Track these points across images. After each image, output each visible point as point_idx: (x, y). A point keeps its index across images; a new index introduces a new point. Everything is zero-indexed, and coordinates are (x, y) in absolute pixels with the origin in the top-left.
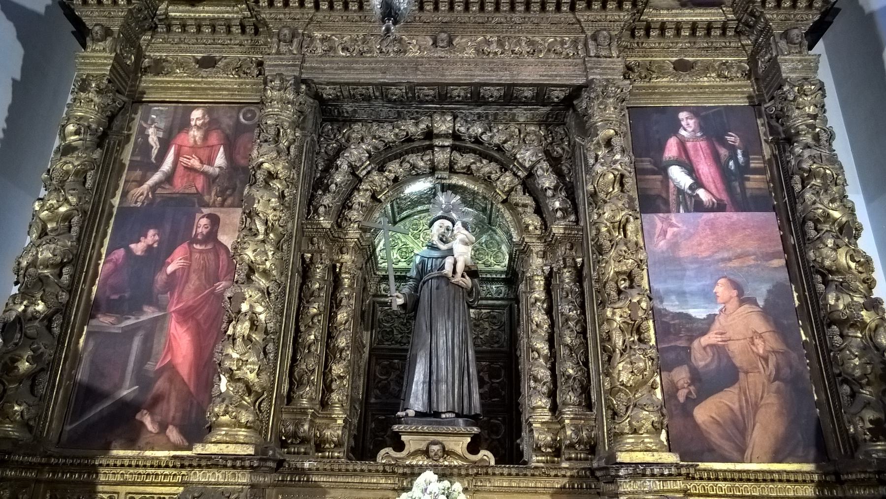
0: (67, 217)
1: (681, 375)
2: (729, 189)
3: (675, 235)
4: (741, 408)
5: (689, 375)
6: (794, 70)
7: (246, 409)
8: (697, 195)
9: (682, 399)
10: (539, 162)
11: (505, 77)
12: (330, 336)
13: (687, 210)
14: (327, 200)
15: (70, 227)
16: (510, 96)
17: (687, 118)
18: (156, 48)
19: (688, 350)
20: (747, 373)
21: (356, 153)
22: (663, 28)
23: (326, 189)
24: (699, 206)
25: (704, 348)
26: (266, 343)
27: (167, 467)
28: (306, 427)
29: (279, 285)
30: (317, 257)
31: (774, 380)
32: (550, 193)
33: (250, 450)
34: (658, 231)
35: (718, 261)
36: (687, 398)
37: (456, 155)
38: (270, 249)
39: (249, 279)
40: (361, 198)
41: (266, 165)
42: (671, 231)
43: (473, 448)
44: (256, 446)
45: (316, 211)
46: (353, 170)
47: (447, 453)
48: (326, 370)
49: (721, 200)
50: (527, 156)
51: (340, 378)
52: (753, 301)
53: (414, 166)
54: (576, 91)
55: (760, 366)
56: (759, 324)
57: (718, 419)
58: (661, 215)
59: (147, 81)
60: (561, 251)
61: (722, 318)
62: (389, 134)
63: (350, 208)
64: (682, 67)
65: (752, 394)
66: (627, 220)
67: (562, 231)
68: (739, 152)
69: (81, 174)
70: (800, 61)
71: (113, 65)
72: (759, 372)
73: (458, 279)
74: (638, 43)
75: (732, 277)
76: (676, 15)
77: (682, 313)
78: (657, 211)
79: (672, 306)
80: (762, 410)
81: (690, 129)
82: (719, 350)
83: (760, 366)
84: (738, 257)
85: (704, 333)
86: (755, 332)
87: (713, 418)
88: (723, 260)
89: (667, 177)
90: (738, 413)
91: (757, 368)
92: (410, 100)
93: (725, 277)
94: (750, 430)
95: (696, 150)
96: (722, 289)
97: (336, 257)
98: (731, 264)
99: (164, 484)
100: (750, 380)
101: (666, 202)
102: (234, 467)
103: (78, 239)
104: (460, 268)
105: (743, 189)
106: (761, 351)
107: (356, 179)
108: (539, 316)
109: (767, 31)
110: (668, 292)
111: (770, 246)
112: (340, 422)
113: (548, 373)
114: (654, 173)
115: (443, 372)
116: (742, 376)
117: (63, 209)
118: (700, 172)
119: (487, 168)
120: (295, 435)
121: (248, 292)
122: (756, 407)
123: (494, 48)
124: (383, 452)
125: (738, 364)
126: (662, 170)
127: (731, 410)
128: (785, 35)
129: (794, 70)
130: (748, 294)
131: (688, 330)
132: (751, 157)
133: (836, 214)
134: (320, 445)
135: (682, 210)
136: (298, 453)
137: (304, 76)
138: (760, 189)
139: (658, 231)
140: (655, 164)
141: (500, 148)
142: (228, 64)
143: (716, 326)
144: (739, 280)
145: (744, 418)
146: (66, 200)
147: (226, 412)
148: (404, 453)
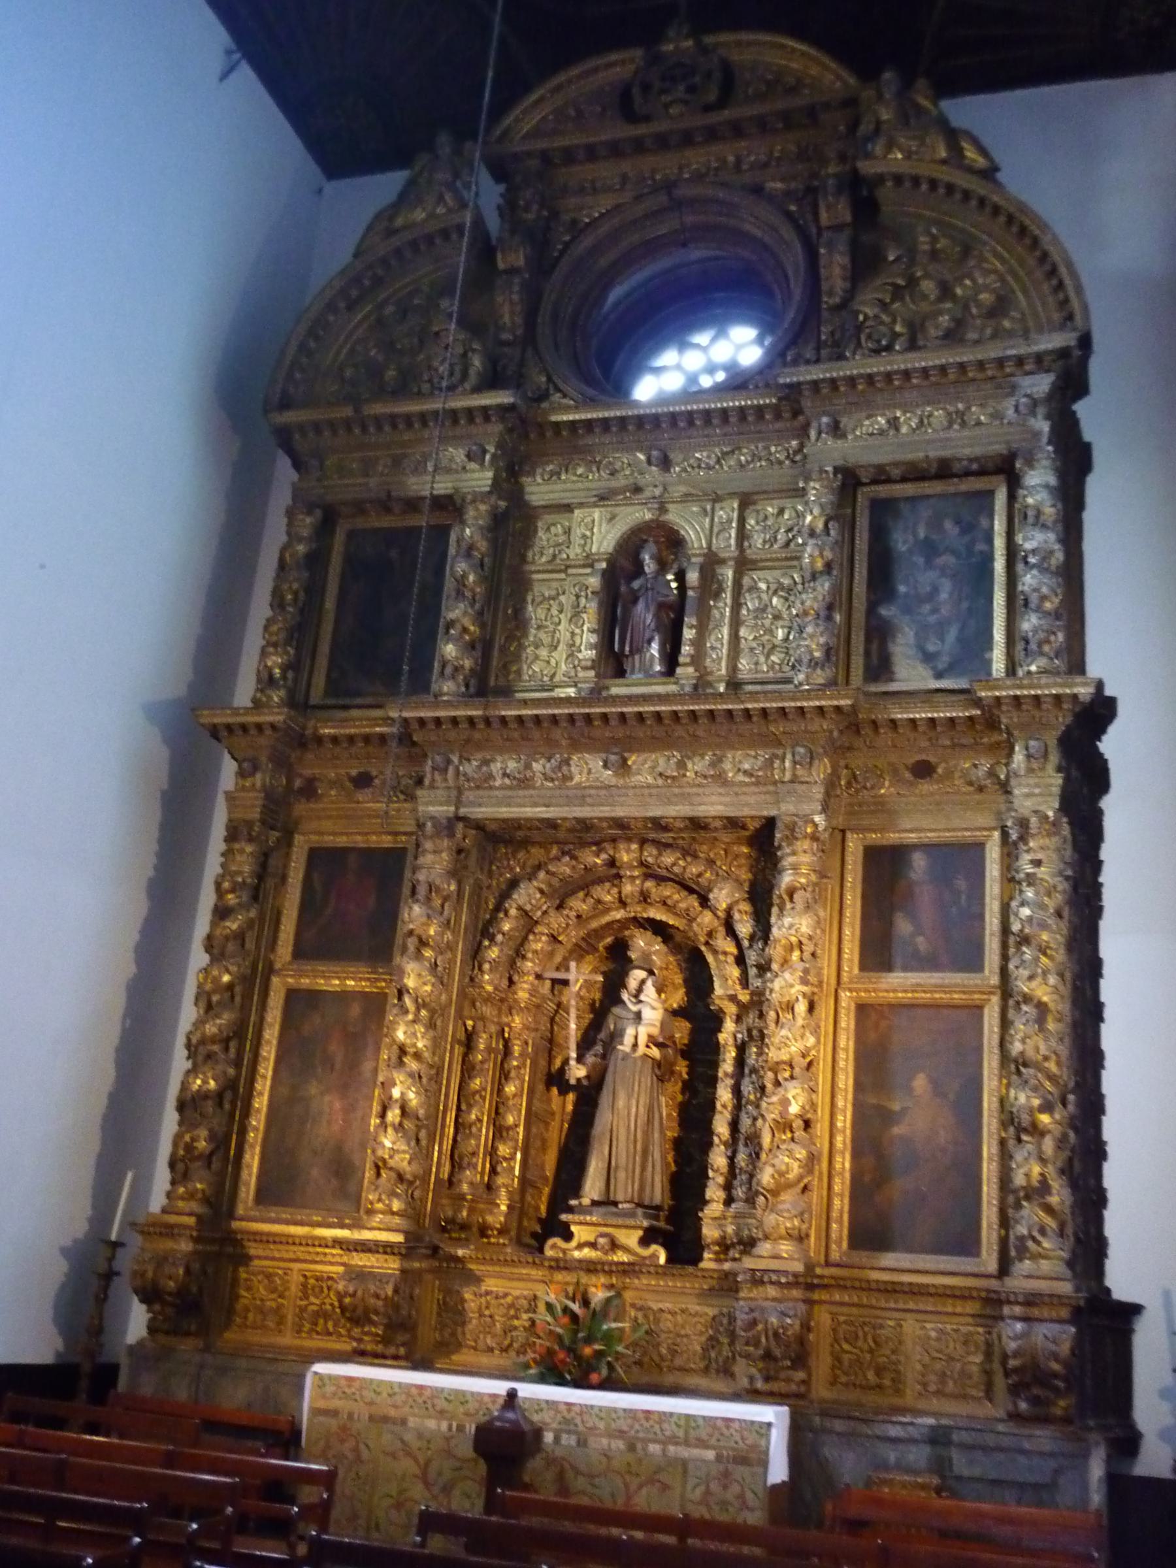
0: (230, 987)
6: (1028, 796)
7: (397, 1195)
10: (737, 902)
11: (684, 810)
12: (497, 1112)
15: (232, 997)
16: (697, 824)
18: (310, 766)
21: (526, 895)
23: (492, 939)
26: (420, 1128)
28: (465, 1213)
29: (431, 1067)
30: (480, 1024)
33: (399, 1238)
38: (420, 1029)
39: (401, 1063)
40: (538, 944)
44: (406, 1233)
45: (480, 969)
46: (524, 913)
47: (614, 1245)
48: (492, 1152)
50: (722, 897)
53: (599, 901)
54: (770, 824)
62: (564, 868)
63: (524, 957)
92: (585, 833)
97: (505, 1020)
99: (332, 1264)
102: (385, 1253)
103: (242, 1007)
107: (529, 923)
117: (226, 978)
120: (451, 1221)
121: (399, 1077)
124: (551, 1242)
134: (483, 1231)
136: (459, 1239)
147: (380, 1200)
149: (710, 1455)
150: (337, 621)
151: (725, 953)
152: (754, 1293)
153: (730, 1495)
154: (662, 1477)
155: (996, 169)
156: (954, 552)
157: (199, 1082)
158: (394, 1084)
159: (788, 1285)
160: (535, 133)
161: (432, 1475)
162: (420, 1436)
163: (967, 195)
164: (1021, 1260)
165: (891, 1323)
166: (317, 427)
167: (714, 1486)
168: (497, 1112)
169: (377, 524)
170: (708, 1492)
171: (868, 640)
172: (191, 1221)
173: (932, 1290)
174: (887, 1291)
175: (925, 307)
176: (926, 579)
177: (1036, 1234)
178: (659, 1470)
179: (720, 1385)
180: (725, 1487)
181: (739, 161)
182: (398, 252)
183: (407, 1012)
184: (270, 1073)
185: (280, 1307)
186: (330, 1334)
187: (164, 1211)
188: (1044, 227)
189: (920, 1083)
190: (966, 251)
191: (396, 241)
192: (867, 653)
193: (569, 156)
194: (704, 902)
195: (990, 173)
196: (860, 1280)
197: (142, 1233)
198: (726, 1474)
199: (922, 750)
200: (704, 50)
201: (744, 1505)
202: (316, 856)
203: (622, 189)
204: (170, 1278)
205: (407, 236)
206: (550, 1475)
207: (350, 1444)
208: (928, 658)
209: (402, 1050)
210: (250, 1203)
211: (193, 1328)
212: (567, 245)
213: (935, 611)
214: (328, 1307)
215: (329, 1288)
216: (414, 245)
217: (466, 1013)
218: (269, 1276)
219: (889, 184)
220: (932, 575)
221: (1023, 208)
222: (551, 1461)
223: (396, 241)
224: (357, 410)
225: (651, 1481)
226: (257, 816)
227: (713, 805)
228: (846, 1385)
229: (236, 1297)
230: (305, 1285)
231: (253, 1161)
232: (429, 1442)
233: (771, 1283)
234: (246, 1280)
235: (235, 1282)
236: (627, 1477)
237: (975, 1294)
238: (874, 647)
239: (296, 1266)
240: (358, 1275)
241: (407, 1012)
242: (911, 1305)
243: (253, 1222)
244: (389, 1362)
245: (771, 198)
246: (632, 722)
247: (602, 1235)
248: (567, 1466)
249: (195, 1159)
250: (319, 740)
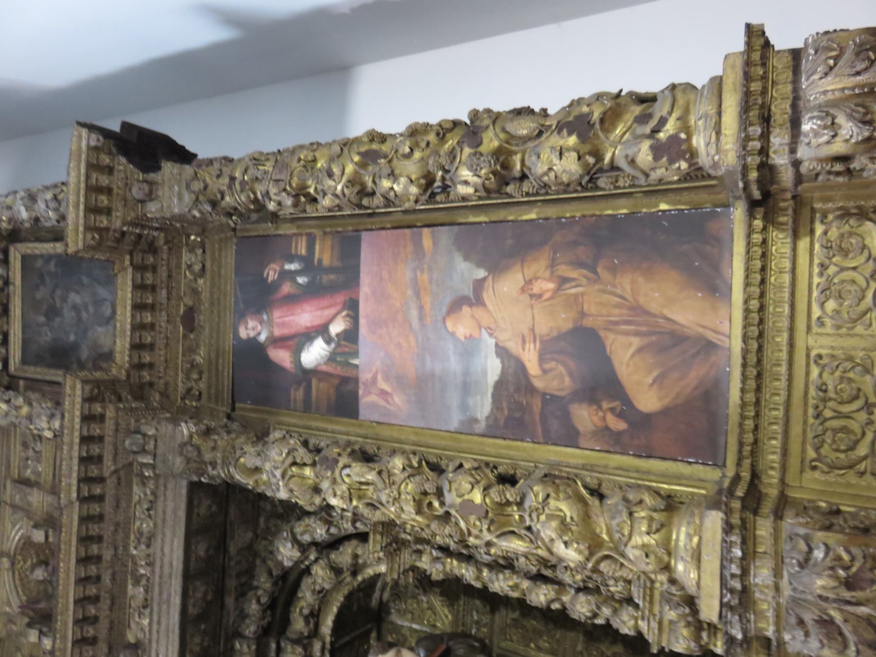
1: (585, 417)
2: (330, 289)
3: (387, 379)
4: (637, 334)
5: (585, 405)
6: (180, 197)
8: (337, 335)
9: (622, 426)
13: (356, 354)
17: (246, 328)
19: (548, 399)
20: (583, 314)
22: (137, 347)
24: (351, 336)
25: (545, 372)
31: (596, 273)
32: (333, 530)
34: (382, 402)
35: (423, 326)
36: (620, 416)
37: (290, 634)
42: (383, 385)
49: (344, 304)
52: (479, 285)
55: (573, 291)
56: (510, 284)
57: (655, 373)
58: (361, 392)
61: (503, 336)
65: (617, 311)
67: (379, 537)
68: (288, 267)
72: (583, 294)
74: (160, 378)
75: (444, 310)
77: (494, 396)
78: (354, 398)
79: (483, 407)
80: (642, 300)
81: (259, 328)
82: (549, 349)
83: (573, 291)
84: (417, 294)
85: (522, 368)
86: (523, 290)
87: (654, 381)
88: (421, 317)
89: (313, 372)
90: (646, 340)
91: (576, 296)
93: (444, 320)
94: (675, 327)
95: (283, 325)
96: (462, 326)
98: (427, 307)
100: (594, 311)
101: (345, 380)
105: (330, 270)
106: (551, 286)
110: (464, 407)
111: (405, 247)
114: (308, 388)
116: (588, 322)
118: (309, 325)
119: (306, 598)
122: (638, 310)
125: (569, 325)
126: (307, 375)
127: (640, 350)
129: (180, 197)
130: (468, 291)
131: (518, 390)
132: (293, 251)
135: (355, 362)
138: (332, 247)
139: (382, 402)
140: (299, 384)
143: (514, 346)
144: (448, 300)
145: (655, 333)
151: (356, 556)
159: (748, 542)
164: (693, 154)
165: (815, 371)
173: (754, 304)
176: (68, 315)
177: (647, 129)
196: (743, 417)
213: (86, 308)
233: (745, 573)
237: (757, 238)
242: (783, 339)
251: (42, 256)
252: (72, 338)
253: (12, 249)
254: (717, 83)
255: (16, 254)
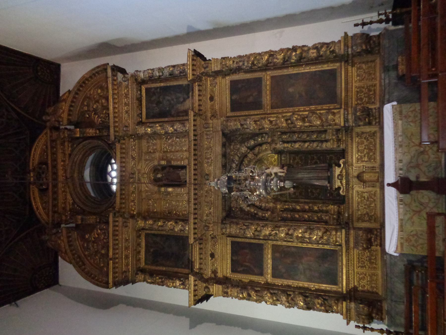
0: (271, 294)
6: (217, 66)
11: (220, 157)
12: (304, 211)
14: (260, 214)
15: (274, 293)
16: (224, 155)
18: (208, 273)
23: (256, 214)
27: (348, 257)
28: (335, 216)
32: (256, 142)
33: (344, 231)
41: (253, 232)
43: (339, 166)
45: (263, 217)
46: (249, 206)
48: (316, 212)
50: (244, 149)
51: (318, 207)
54: (224, 135)
59: (220, 275)
60: (276, 138)
64: (212, 99)
66: (269, 120)
69: (256, 291)
70: (214, 64)
71: (218, 284)
73: (285, 171)
76: (196, 101)
97: (278, 210)
99: (354, 258)
102: (349, 235)
104: (281, 170)
108: (297, 145)
109: (202, 74)
112: (332, 206)
113: (315, 143)
115: (316, 175)
117: (269, 295)
121: (295, 234)
123: (210, 161)
128: (205, 68)
129: (217, 66)
133: (266, 57)
134: (339, 213)
137: (220, 221)
141: (240, 158)
142: (213, 249)
146: (266, 294)
148: (341, 187)
149: (400, 122)
150: (168, 266)
151: (259, 150)
152: (351, 121)
153: (412, 115)
154: (409, 135)
155: (69, 90)
156: (159, 97)
157: (300, 303)
158: (298, 236)
159: (348, 111)
160: (48, 215)
161: (418, 209)
162: (405, 214)
163: (74, 97)
166: (114, 273)
167: (410, 120)
168: (304, 211)
169: (144, 256)
170: (412, 122)
171: (179, 116)
172: (344, 303)
174: (347, 91)
175: (100, 107)
177: (328, 49)
178: (407, 137)
179: (378, 135)
180: (410, 117)
181: (62, 161)
182: (71, 251)
183: (276, 233)
184: (298, 282)
185: (369, 275)
186: (376, 258)
187: (342, 314)
188: (83, 77)
189: (291, 90)
190: (89, 98)
191: (68, 251)
192: (183, 116)
193: (55, 206)
194: (245, 156)
195: (69, 91)
197: (350, 321)
198: (405, 117)
199: (207, 99)
200: (34, 170)
201: (414, 110)
202: (234, 270)
203: (66, 192)
204: (364, 309)
205: (67, 247)
206: (413, 171)
207: (411, 237)
208: (184, 100)
209: (287, 234)
210: (337, 287)
211: (379, 304)
212: (77, 206)
213: (173, 99)
214: (368, 258)
215: (362, 258)
216: (70, 246)
217: (276, 220)
218: (360, 279)
219: (70, 117)
220: (164, 102)
221: (78, 82)
222: (408, 171)
223: (68, 251)
224: (111, 259)
225: (411, 139)
226: (221, 286)
227: (218, 149)
228: (375, 99)
229: (368, 292)
230: (362, 267)
231: (324, 286)
232: (407, 211)
233: (347, 117)
234: (362, 287)
235: (363, 291)
236: (411, 146)
238: (181, 114)
239: (356, 270)
240: (356, 244)
241: (276, 233)
243: (344, 285)
244: (383, 235)
245: (72, 151)
246: (196, 172)
247: (338, 178)
248: (409, 166)
249: (325, 304)
250: (200, 269)
251: (154, 88)
252: (168, 109)
253: (142, 86)
254: (340, 41)
255: (143, 88)
